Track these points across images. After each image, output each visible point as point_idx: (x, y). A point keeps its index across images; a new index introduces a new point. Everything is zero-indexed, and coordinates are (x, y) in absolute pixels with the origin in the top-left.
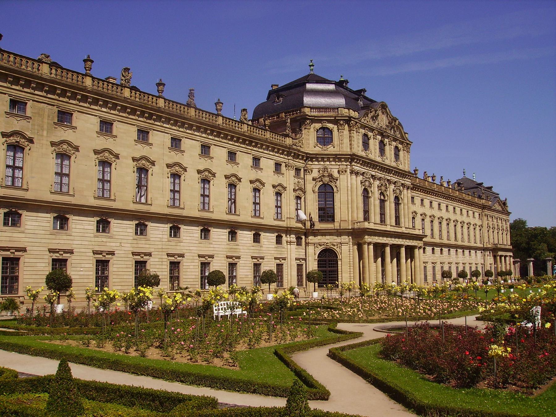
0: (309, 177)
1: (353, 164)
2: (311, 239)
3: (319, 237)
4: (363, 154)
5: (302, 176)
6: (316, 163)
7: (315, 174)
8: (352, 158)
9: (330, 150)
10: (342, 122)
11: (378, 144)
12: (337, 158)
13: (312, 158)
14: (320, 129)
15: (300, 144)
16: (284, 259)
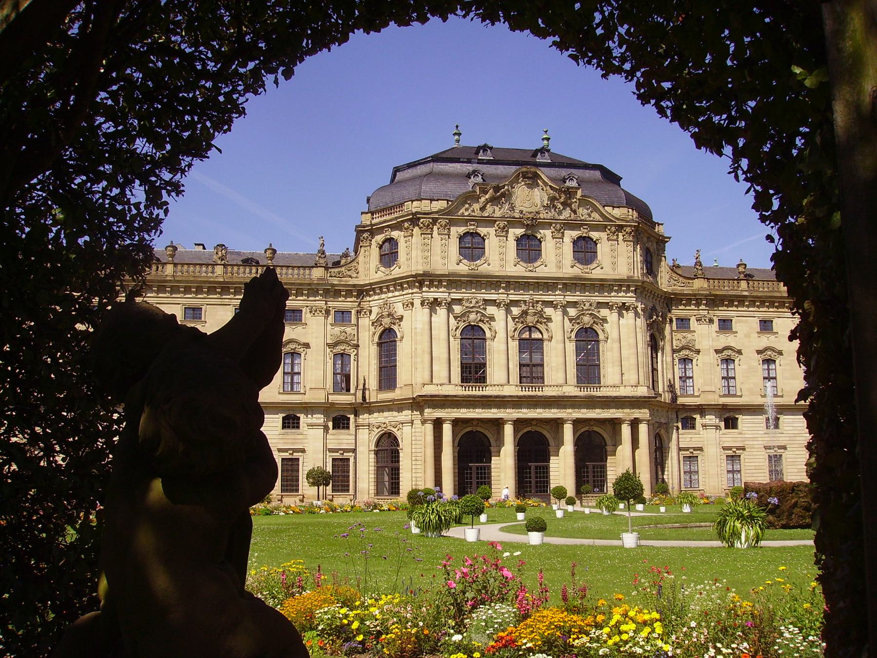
0: (365, 322)
1: (424, 289)
2: (364, 418)
3: (376, 415)
4: (464, 268)
5: (354, 321)
6: (376, 297)
7: (373, 317)
8: (422, 280)
9: (396, 272)
10: (406, 225)
11: (512, 244)
12: (398, 284)
13: (367, 291)
14: (384, 243)
15: (349, 273)
16: (303, 451)
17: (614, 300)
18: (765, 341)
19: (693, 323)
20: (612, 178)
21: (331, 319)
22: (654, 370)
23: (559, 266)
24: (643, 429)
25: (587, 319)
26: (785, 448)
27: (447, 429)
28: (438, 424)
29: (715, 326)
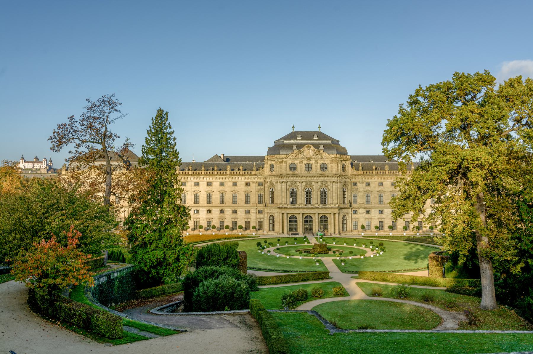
0: (266, 185)
8: (281, 176)
11: (303, 165)
17: (331, 180)
18: (381, 188)
19: (358, 184)
20: (336, 143)
21: (257, 184)
22: (344, 198)
23: (316, 172)
24: (337, 216)
25: (324, 186)
26: (384, 219)
27: (285, 215)
28: (283, 214)
29: (364, 184)
